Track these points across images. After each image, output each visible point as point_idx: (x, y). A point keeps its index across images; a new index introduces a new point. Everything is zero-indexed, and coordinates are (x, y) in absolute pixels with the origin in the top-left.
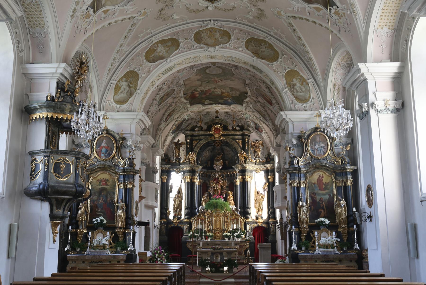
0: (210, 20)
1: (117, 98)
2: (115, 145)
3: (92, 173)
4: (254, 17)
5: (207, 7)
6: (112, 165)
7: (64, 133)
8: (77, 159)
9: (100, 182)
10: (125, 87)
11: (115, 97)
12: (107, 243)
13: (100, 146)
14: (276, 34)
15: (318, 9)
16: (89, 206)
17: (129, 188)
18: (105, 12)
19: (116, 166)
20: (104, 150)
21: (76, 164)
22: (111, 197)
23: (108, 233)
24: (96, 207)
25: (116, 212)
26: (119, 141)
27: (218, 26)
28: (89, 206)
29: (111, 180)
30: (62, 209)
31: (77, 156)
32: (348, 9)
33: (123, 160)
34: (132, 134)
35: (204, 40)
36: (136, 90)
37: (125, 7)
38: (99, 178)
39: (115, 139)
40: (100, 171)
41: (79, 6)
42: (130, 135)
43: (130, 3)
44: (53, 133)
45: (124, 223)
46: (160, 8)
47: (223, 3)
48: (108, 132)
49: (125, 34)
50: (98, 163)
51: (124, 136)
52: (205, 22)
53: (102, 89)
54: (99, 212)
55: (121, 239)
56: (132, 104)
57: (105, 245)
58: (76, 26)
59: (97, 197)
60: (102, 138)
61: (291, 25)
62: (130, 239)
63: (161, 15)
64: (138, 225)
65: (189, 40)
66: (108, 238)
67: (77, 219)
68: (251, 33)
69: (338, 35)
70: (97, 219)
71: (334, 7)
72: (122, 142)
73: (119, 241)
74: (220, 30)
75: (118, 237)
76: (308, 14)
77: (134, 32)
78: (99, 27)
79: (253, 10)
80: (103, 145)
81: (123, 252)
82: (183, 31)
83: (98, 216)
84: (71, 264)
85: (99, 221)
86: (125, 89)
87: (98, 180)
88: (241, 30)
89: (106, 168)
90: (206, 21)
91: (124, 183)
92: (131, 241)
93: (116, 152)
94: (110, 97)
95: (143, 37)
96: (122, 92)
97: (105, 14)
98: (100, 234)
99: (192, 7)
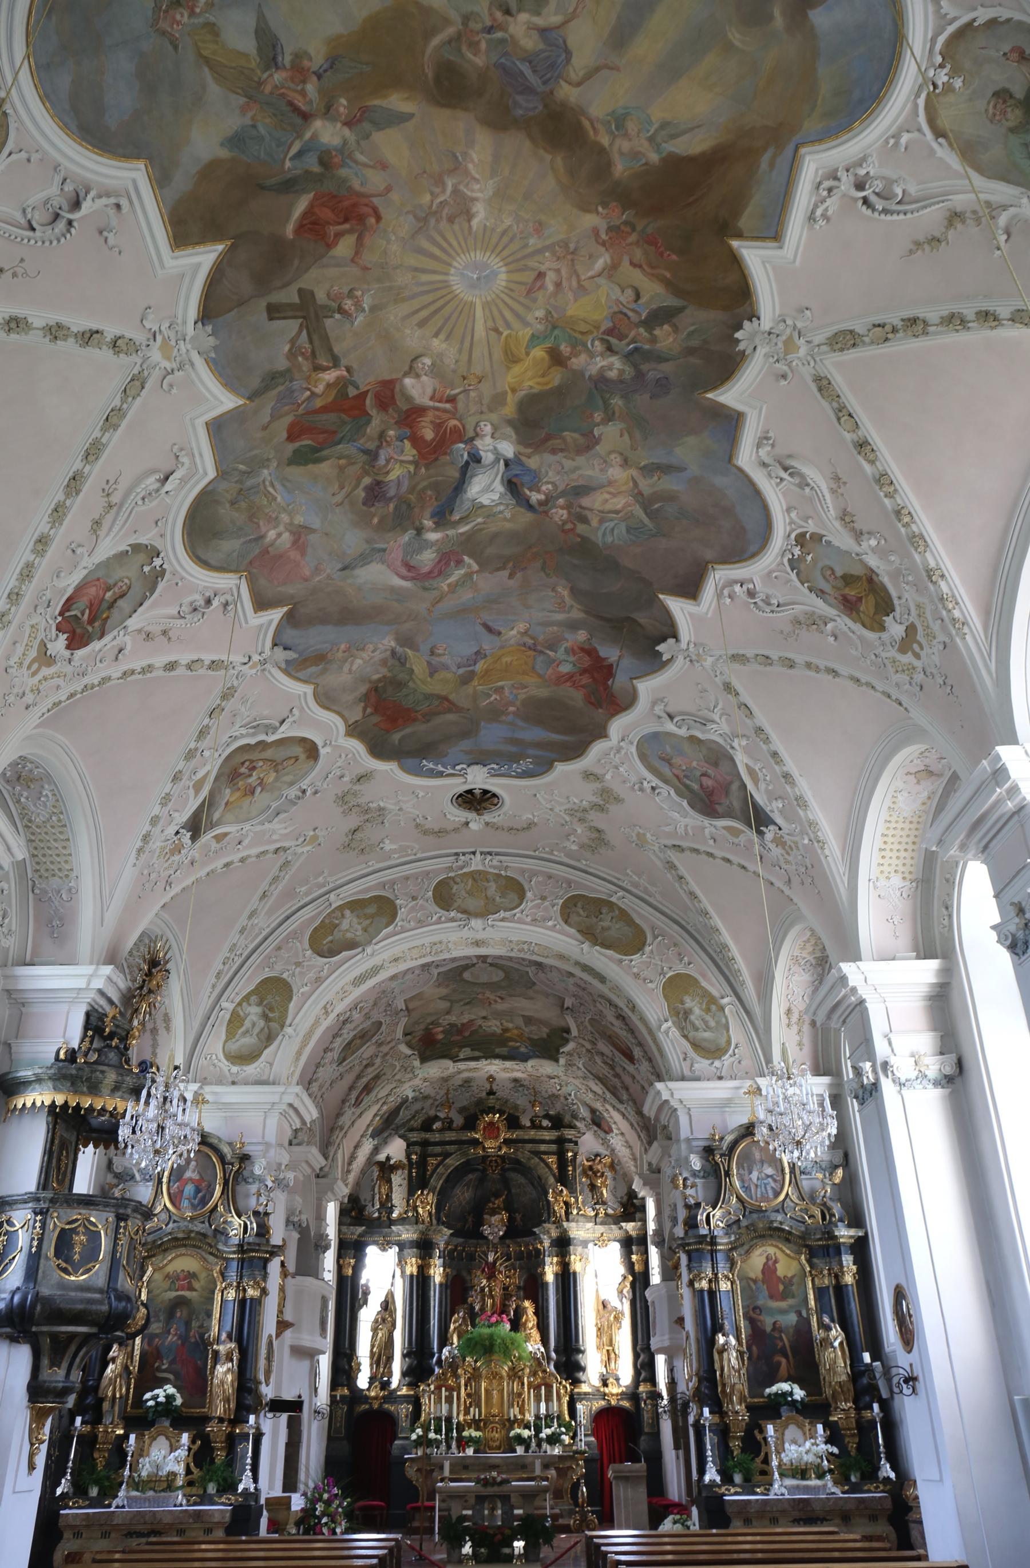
0: (474, 853)
1: (234, 1047)
2: (219, 1174)
3: (154, 1256)
4: (582, 846)
5: (467, 823)
6: (210, 1233)
7: (91, 1146)
8: (120, 1218)
9: (174, 1279)
10: (254, 1018)
11: (229, 1043)
14: (636, 885)
15: (734, 832)
16: (137, 1352)
17: (252, 1299)
18: (219, 838)
19: (221, 1233)
20: (189, 1189)
21: (117, 1232)
22: (201, 1327)
23: (185, 1438)
24: (158, 1355)
25: (212, 1373)
26: (232, 1164)
27: (495, 867)
28: (137, 1352)
29: (203, 1276)
30: (65, 1365)
31: (121, 1211)
32: (803, 833)
34: (268, 1145)
35: (459, 902)
36: (282, 1027)
37: (267, 825)
38: (170, 1269)
40: (175, 1247)
41: (159, 828)
42: (260, 1148)
43: (282, 816)
44: (63, 1145)
45: (233, 1405)
46: (353, 827)
47: (505, 814)
48: (205, 1140)
49: (264, 886)
50: (171, 1225)
51: (248, 1149)
52: (462, 858)
53: (196, 1024)
54: (165, 1371)
55: (220, 1456)
56: (271, 1065)
58: (146, 872)
59: (161, 1325)
61: (671, 866)
62: (245, 1457)
63: (354, 843)
64: (270, 1411)
65: (421, 902)
66: (182, 1453)
67: (100, 1394)
68: (576, 882)
69: (787, 891)
70: (156, 1391)
71: (771, 827)
73: (213, 1461)
74: (499, 876)
75: (213, 1449)
76: (711, 842)
77: (285, 881)
78: (203, 873)
79: (579, 831)
80: (188, 1174)
81: (223, 1500)
82: (407, 878)
83: (160, 1383)
84: (68, 1540)
86: (254, 1025)
87: (168, 1276)
88: (550, 877)
89: (193, 1239)
90: (464, 854)
91: (239, 1283)
92: (249, 1461)
94: (215, 1045)
95: (307, 894)
96: (247, 1031)
97: (218, 842)
98: (162, 1441)
99: (431, 824)
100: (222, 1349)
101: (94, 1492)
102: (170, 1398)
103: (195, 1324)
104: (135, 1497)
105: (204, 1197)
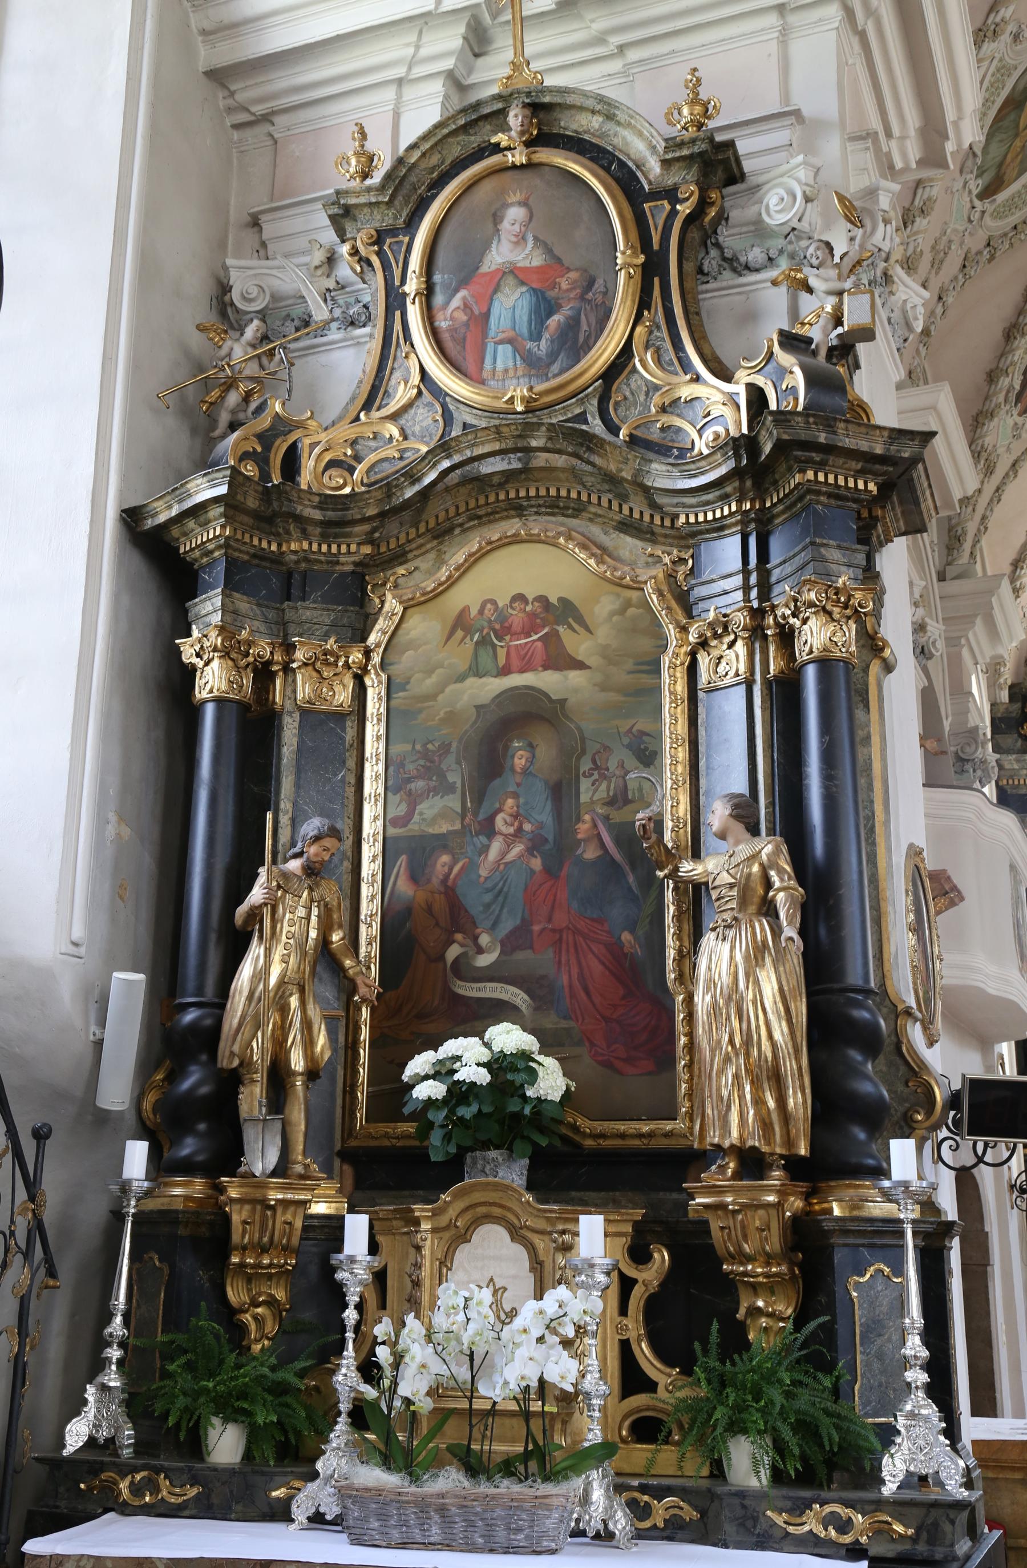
3: (400, 557)
9: (486, 634)
12: (583, 1373)
13: (467, 273)
17: (825, 663)
20: (510, 307)
22: (621, 799)
23: (593, 1235)
24: (456, 917)
25: (687, 976)
28: (370, 905)
29: (602, 608)
33: (725, 375)
38: (468, 595)
39: (625, 179)
40: (481, 518)
45: (798, 1100)
48: (547, 119)
54: (489, 975)
55: (769, 1315)
57: (546, 1408)
60: (487, 188)
66: (582, 1303)
70: (451, 1047)
72: (703, 204)
73: (735, 1341)
75: (729, 1288)
80: (500, 254)
81: (811, 1524)
83: (474, 1018)
87: (461, 622)
91: (758, 614)
92: (915, 1346)
93: (644, 304)
100: (714, 867)
101: (226, 1445)
102: (508, 1070)
103: (590, 792)
104: (377, 1492)
105: (572, 325)
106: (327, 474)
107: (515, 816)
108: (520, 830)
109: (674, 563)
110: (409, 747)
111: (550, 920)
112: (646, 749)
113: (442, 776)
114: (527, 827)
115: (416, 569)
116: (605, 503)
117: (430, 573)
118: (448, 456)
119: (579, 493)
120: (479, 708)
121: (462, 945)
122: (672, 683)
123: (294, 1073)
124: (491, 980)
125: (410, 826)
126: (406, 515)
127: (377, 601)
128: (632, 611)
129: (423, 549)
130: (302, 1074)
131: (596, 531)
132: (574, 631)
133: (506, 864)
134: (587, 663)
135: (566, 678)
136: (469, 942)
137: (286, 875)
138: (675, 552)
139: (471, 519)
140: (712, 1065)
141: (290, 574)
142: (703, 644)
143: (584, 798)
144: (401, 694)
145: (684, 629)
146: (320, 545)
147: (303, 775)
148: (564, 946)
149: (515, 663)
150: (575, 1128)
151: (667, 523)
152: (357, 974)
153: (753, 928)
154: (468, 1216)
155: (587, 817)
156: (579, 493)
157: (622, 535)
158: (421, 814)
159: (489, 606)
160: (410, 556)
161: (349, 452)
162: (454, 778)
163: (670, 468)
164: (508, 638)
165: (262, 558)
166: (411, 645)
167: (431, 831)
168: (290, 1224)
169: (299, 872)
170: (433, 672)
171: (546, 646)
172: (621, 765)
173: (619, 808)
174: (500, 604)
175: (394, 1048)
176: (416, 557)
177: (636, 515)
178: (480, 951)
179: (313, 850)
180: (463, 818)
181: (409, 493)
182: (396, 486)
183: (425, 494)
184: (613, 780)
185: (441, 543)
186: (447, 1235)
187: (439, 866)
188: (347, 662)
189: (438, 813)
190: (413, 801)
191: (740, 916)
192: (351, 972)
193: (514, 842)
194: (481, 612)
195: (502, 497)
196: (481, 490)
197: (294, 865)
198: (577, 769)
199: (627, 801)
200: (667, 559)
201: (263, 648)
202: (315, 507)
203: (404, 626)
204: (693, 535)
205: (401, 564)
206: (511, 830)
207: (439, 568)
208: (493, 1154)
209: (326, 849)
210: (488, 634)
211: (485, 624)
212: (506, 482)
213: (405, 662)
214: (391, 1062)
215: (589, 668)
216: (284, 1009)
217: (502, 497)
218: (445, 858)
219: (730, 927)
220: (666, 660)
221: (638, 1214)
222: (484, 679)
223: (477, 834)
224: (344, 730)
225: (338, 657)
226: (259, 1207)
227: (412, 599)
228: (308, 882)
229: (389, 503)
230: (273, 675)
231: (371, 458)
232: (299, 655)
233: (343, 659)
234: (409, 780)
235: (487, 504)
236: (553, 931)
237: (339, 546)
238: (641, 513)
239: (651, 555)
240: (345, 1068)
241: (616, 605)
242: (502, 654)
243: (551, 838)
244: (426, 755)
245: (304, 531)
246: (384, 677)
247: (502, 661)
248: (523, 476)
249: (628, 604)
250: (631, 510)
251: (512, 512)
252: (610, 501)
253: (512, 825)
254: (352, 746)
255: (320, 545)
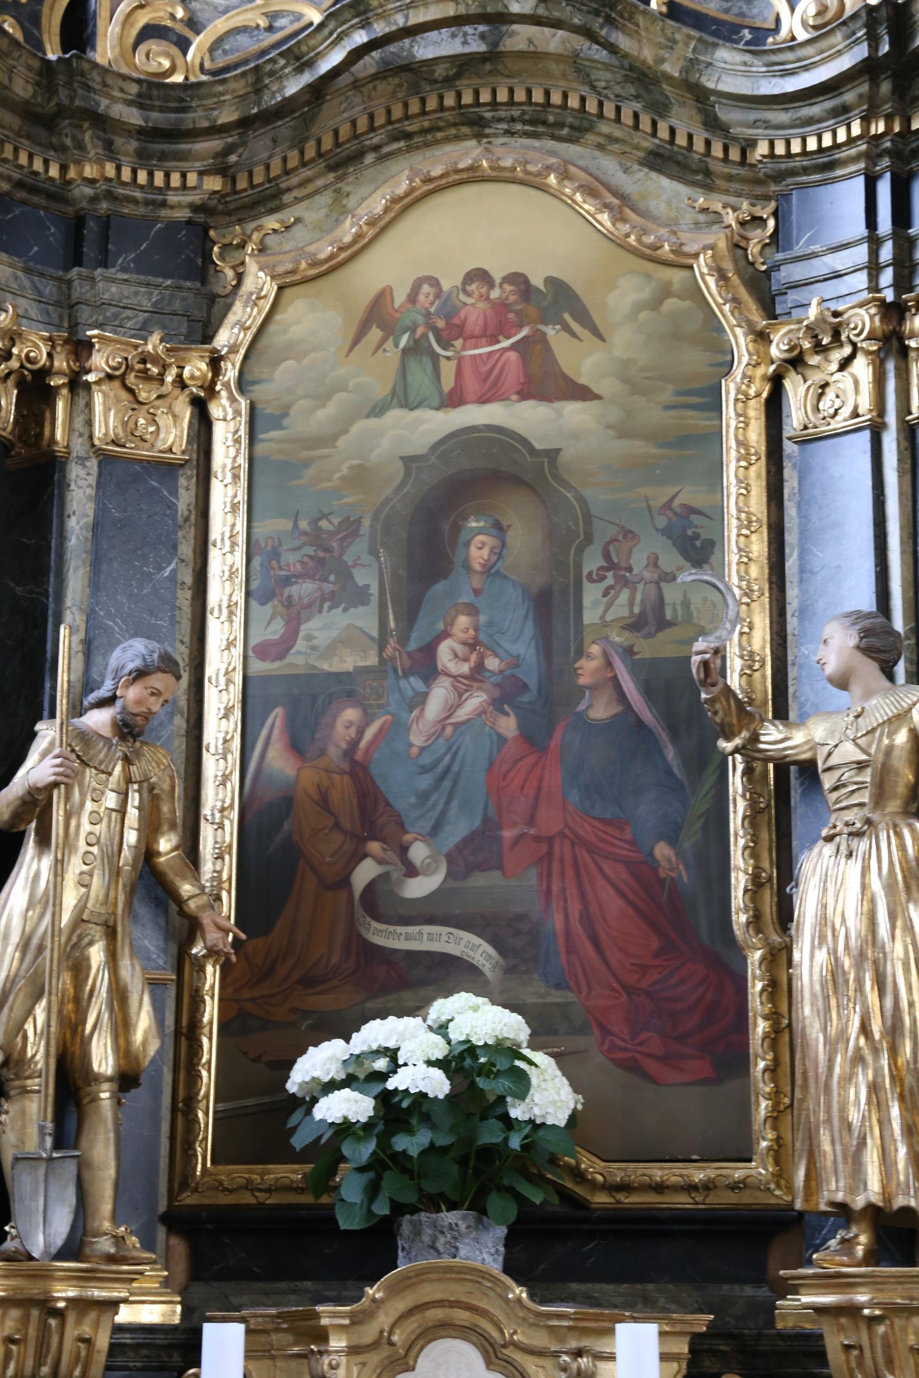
3: (269, 199)
9: (422, 336)
22: (651, 620)
24: (369, 815)
28: (219, 792)
29: (622, 296)
38: (389, 268)
40: (408, 138)
70: (375, 1033)
83: (411, 983)
85: (420, 1078)
87: (377, 315)
100: (823, 733)
106: (143, 48)
107: (472, 645)
108: (479, 667)
109: (742, 224)
110: (288, 525)
111: (531, 821)
112: (696, 536)
113: (345, 575)
114: (492, 663)
115: (298, 220)
116: (627, 118)
117: (323, 229)
118: (365, 25)
119: (583, 100)
120: (408, 460)
121: (380, 862)
122: (740, 425)
123: (98, 1079)
124: (431, 920)
125: (289, 659)
126: (284, 127)
127: (230, 273)
128: (671, 304)
129: (310, 188)
130: (109, 1079)
131: (609, 166)
132: (573, 334)
133: (457, 725)
134: (595, 389)
135: (560, 415)
136: (392, 856)
137: (86, 738)
138: (745, 205)
139: (395, 139)
140: (830, 1068)
141: (80, 221)
142: (796, 362)
143: (590, 616)
144: (273, 434)
145: (762, 337)
146: (134, 172)
147: (104, 567)
148: (556, 866)
149: (471, 386)
150: (578, 1175)
151: (735, 155)
152: (202, 908)
153: (899, 835)
154: (413, 1325)
155: (595, 649)
156: (583, 100)
157: (654, 175)
158: (309, 638)
159: (426, 288)
160: (287, 198)
161: (180, 13)
162: (366, 577)
163: (748, 58)
164: (458, 343)
165: (33, 190)
166: (291, 351)
167: (326, 667)
168: (88, 1341)
169: (107, 732)
170: (329, 397)
171: (525, 361)
172: (654, 562)
173: (650, 635)
174: (446, 286)
175: (265, 1033)
176: (298, 200)
177: (681, 141)
178: (412, 871)
179: (133, 693)
180: (381, 649)
181: (293, 86)
182: (272, 74)
183: (318, 91)
184: (640, 587)
185: (340, 179)
186: (374, 1358)
187: (339, 727)
188: (180, 376)
189: (340, 638)
190: (295, 615)
191: (875, 817)
192: (192, 905)
193: (469, 688)
194: (412, 298)
195: (449, 101)
196: (415, 89)
197: (98, 720)
198: (579, 567)
199: (663, 624)
200: (730, 218)
201: (35, 347)
202: (130, 103)
203: (278, 317)
204: (779, 177)
205: (272, 211)
206: (465, 668)
207: (338, 222)
208: (449, 1217)
209: (156, 693)
210: (425, 336)
211: (420, 319)
212: (458, 75)
213: (278, 381)
214: (257, 1060)
215: (597, 397)
216: (79, 968)
217: (449, 101)
218: (351, 714)
219: (859, 834)
220: (730, 389)
221: (702, 1322)
222: (417, 413)
223: (406, 675)
224: (174, 492)
225: (165, 367)
226: (35, 1313)
227: (293, 272)
228: (120, 750)
229: (258, 103)
230: (50, 395)
231: (220, 25)
232: (100, 360)
233: (174, 371)
234: (287, 581)
235: (424, 113)
236: (538, 839)
237: (167, 176)
238: (690, 137)
239: (704, 210)
240: (176, 1071)
241: (645, 294)
242: (448, 370)
243: (533, 681)
244: (316, 538)
245: (108, 145)
246: (244, 404)
247: (448, 383)
248: (488, 67)
249: (665, 292)
250: (672, 131)
251: (465, 130)
252: (636, 116)
253: (466, 660)
254: (187, 520)
255: (134, 172)
